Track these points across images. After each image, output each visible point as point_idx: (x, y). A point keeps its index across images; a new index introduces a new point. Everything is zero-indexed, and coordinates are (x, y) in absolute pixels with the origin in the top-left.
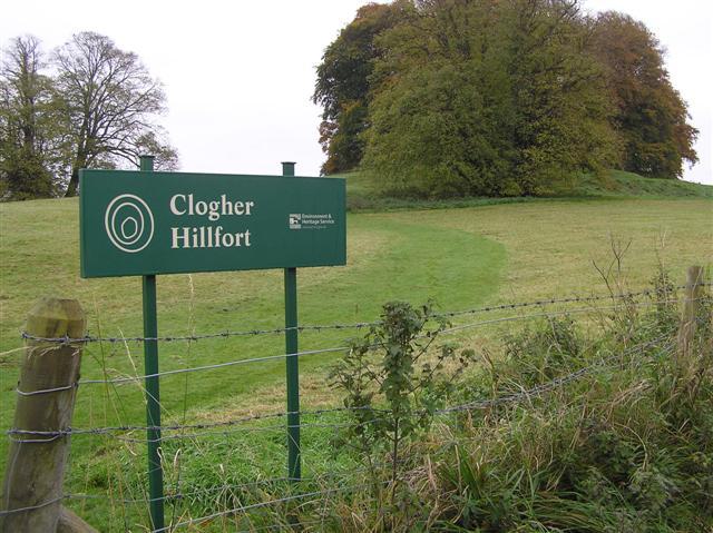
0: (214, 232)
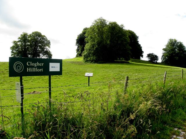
0: (35, 68)
